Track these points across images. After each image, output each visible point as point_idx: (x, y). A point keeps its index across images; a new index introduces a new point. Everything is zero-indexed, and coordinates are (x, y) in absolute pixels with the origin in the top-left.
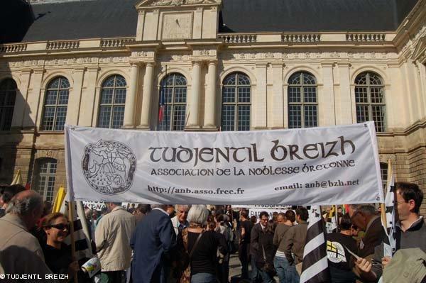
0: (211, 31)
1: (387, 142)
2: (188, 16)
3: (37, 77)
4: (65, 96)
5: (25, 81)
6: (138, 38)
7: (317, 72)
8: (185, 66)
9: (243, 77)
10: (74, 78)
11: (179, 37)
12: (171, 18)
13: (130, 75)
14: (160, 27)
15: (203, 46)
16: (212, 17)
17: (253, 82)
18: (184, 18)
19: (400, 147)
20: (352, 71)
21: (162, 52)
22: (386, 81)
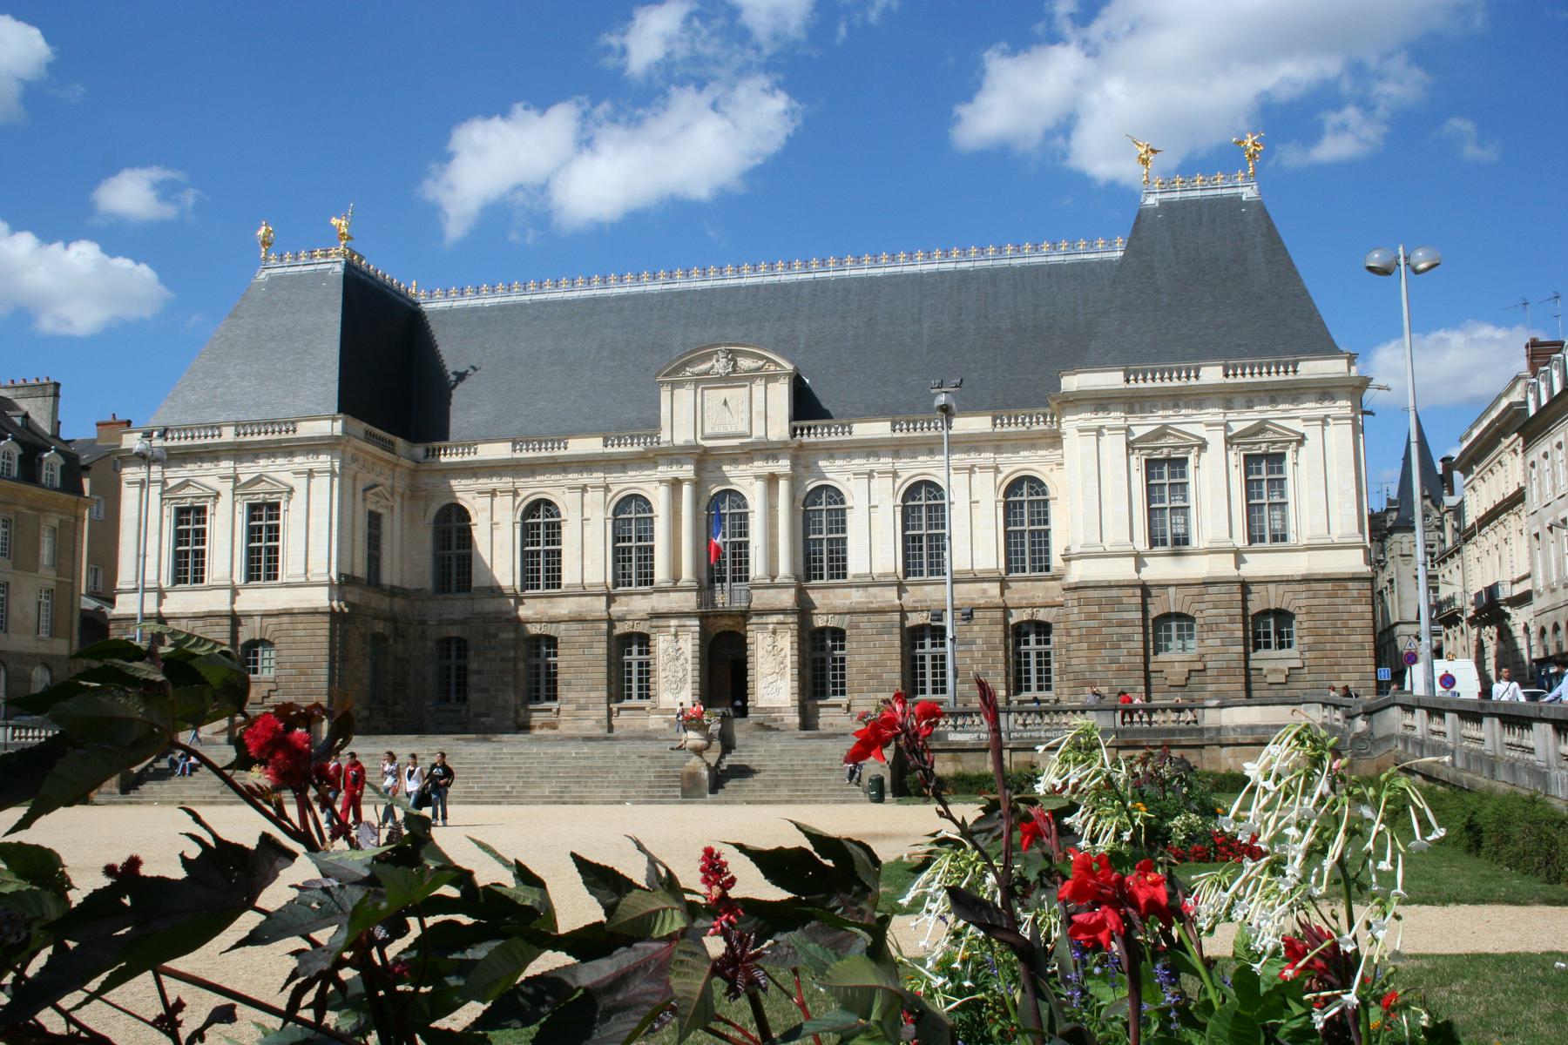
0: (779, 428)
1: (1047, 588)
2: (745, 391)
3: (504, 504)
4: (554, 531)
5: (484, 510)
6: (665, 436)
8: (745, 480)
9: (836, 495)
10: (567, 503)
11: (731, 430)
12: (714, 397)
13: (659, 498)
14: (699, 415)
15: (767, 451)
16: (780, 394)
17: (849, 503)
18: (737, 395)
20: (1001, 477)
21: (705, 459)
22: (1052, 492)
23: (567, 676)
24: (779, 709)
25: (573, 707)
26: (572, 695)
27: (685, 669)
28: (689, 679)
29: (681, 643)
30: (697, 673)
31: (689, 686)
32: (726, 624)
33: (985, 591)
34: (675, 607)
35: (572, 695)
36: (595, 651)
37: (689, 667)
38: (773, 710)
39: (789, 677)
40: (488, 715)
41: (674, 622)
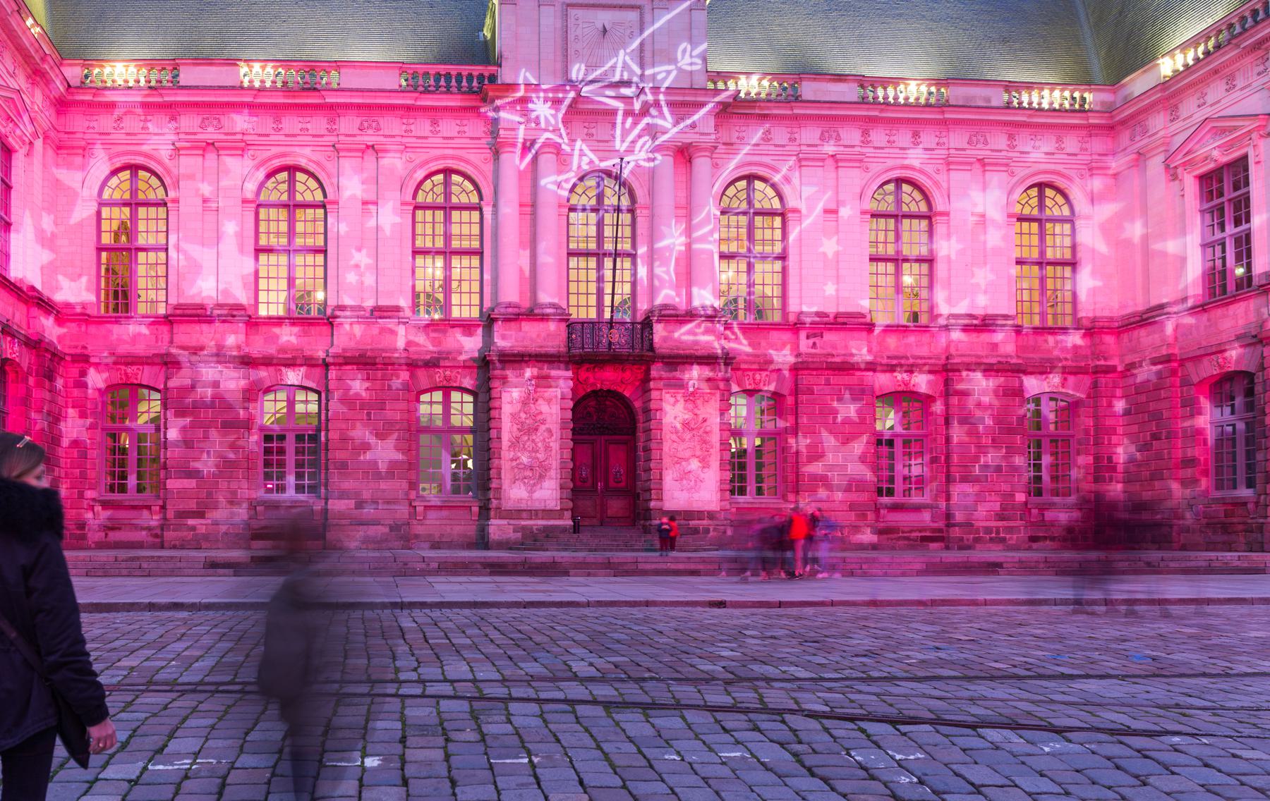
5: (191, 177)
7: (936, 183)
19: (1105, 359)
23: (340, 455)
24: (699, 514)
25: (352, 503)
26: (348, 484)
27: (547, 448)
28: (555, 463)
30: (567, 454)
31: (554, 473)
32: (607, 378)
33: (995, 346)
34: (533, 348)
35: (348, 484)
36: (389, 414)
37: (555, 446)
38: (689, 514)
39: (715, 463)
40: (201, 515)
41: (528, 373)
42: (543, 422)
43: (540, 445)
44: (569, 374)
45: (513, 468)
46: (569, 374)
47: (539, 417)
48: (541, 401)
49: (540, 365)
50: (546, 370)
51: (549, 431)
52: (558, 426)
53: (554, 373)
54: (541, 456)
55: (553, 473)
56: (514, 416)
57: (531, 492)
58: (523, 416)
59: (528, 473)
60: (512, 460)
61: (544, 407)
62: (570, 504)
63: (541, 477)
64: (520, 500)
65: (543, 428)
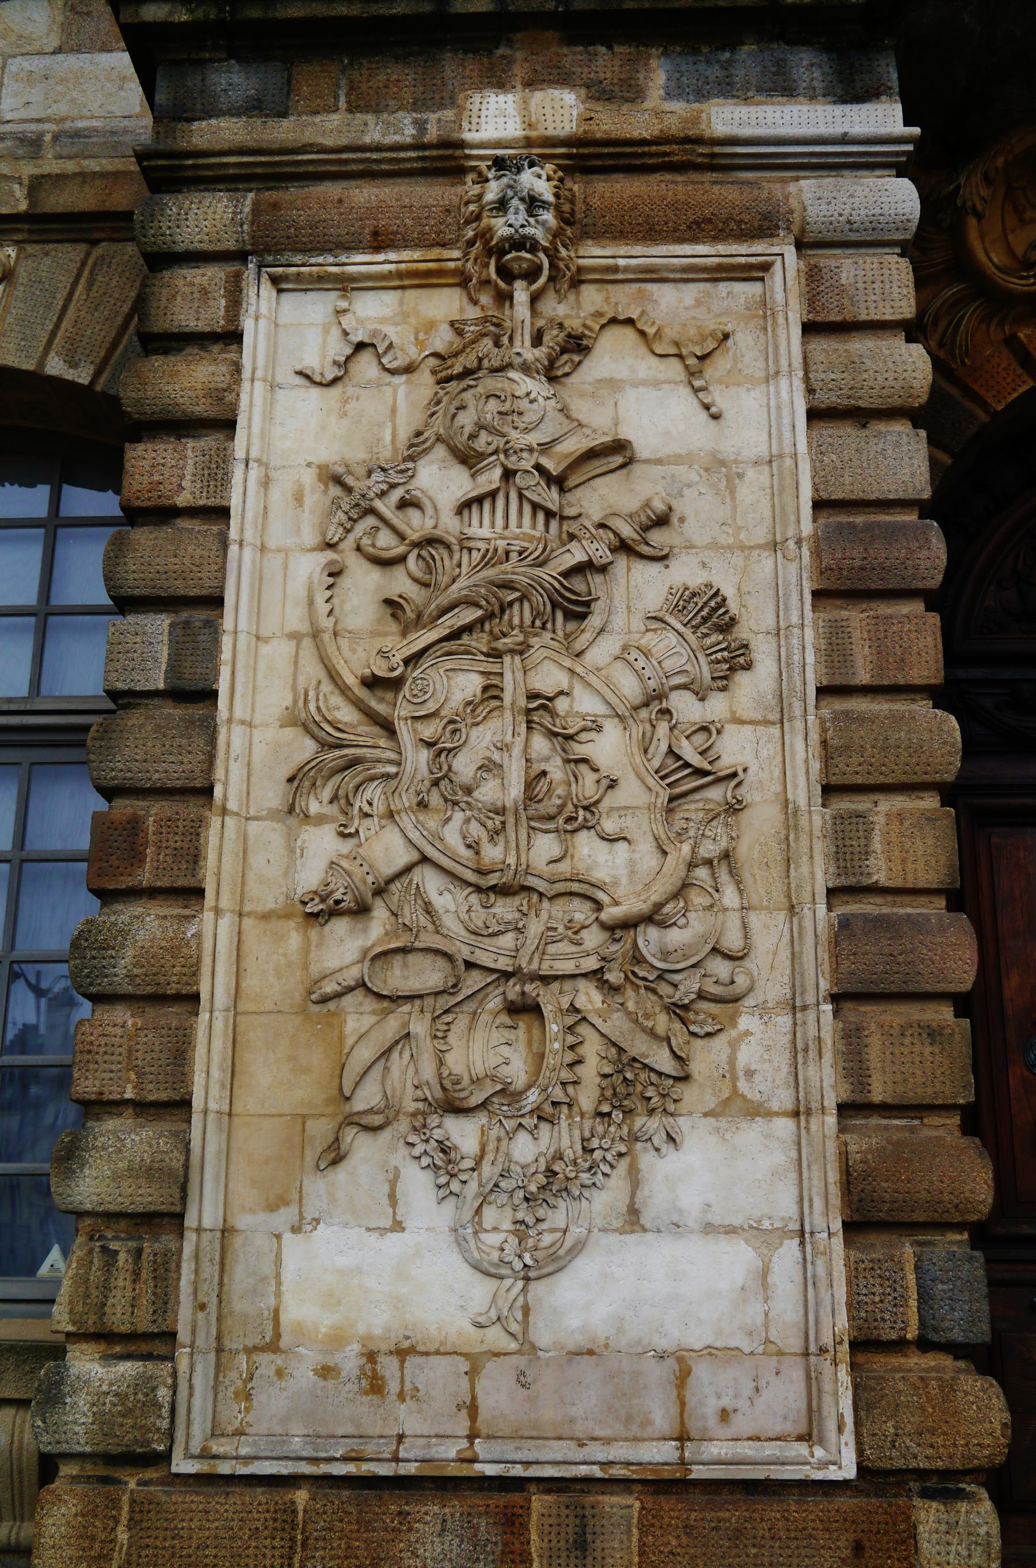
27: (690, 778)
29: (633, 397)
30: (910, 842)
31: (769, 1045)
37: (769, 748)
42: (643, 539)
43: (609, 748)
44: (884, 119)
45: (322, 1000)
46: (884, 119)
47: (601, 498)
48: (613, 357)
49: (605, 63)
50: (659, 103)
51: (709, 615)
52: (798, 575)
53: (728, 118)
54: (623, 865)
55: (757, 1047)
56: (357, 500)
57: (537, 1265)
58: (441, 482)
59: (487, 1049)
60: (322, 911)
61: (633, 397)
62: (983, 1413)
63: (637, 1095)
64: (382, 1366)
65: (638, 591)
